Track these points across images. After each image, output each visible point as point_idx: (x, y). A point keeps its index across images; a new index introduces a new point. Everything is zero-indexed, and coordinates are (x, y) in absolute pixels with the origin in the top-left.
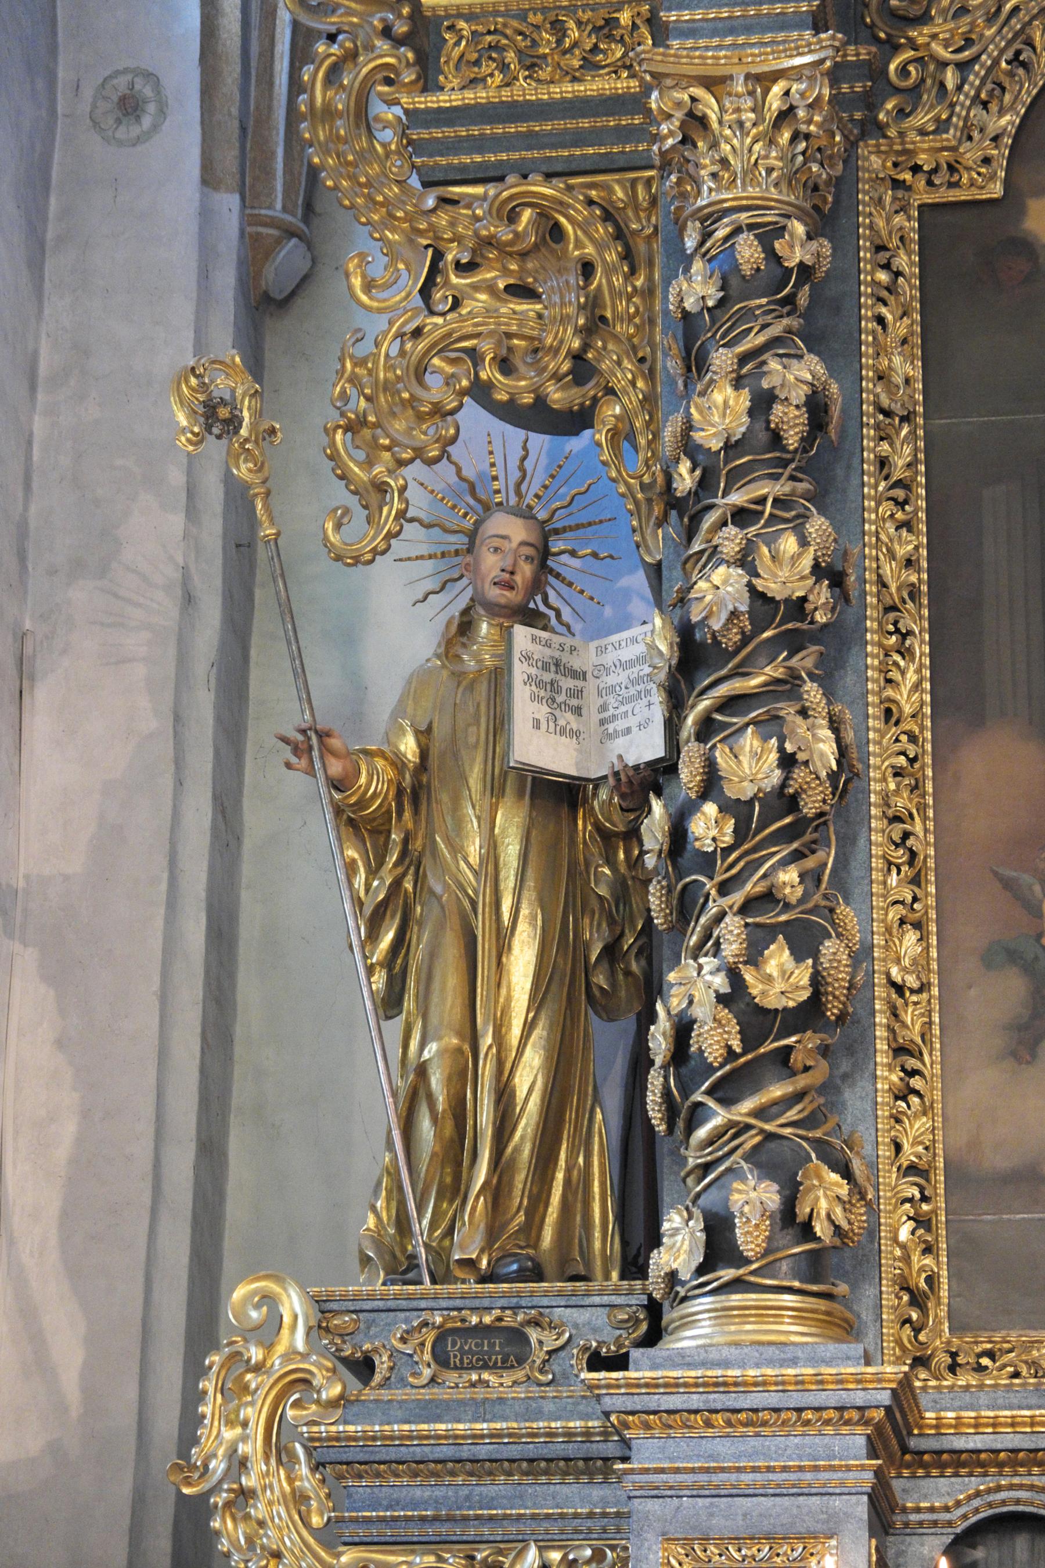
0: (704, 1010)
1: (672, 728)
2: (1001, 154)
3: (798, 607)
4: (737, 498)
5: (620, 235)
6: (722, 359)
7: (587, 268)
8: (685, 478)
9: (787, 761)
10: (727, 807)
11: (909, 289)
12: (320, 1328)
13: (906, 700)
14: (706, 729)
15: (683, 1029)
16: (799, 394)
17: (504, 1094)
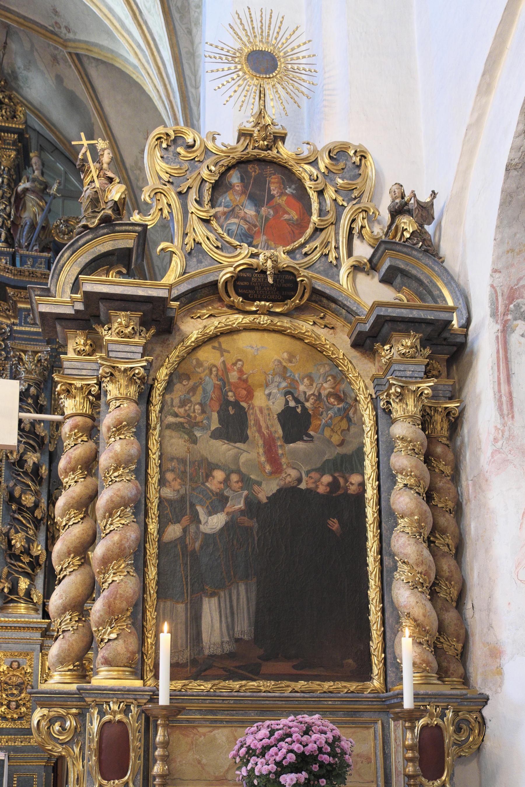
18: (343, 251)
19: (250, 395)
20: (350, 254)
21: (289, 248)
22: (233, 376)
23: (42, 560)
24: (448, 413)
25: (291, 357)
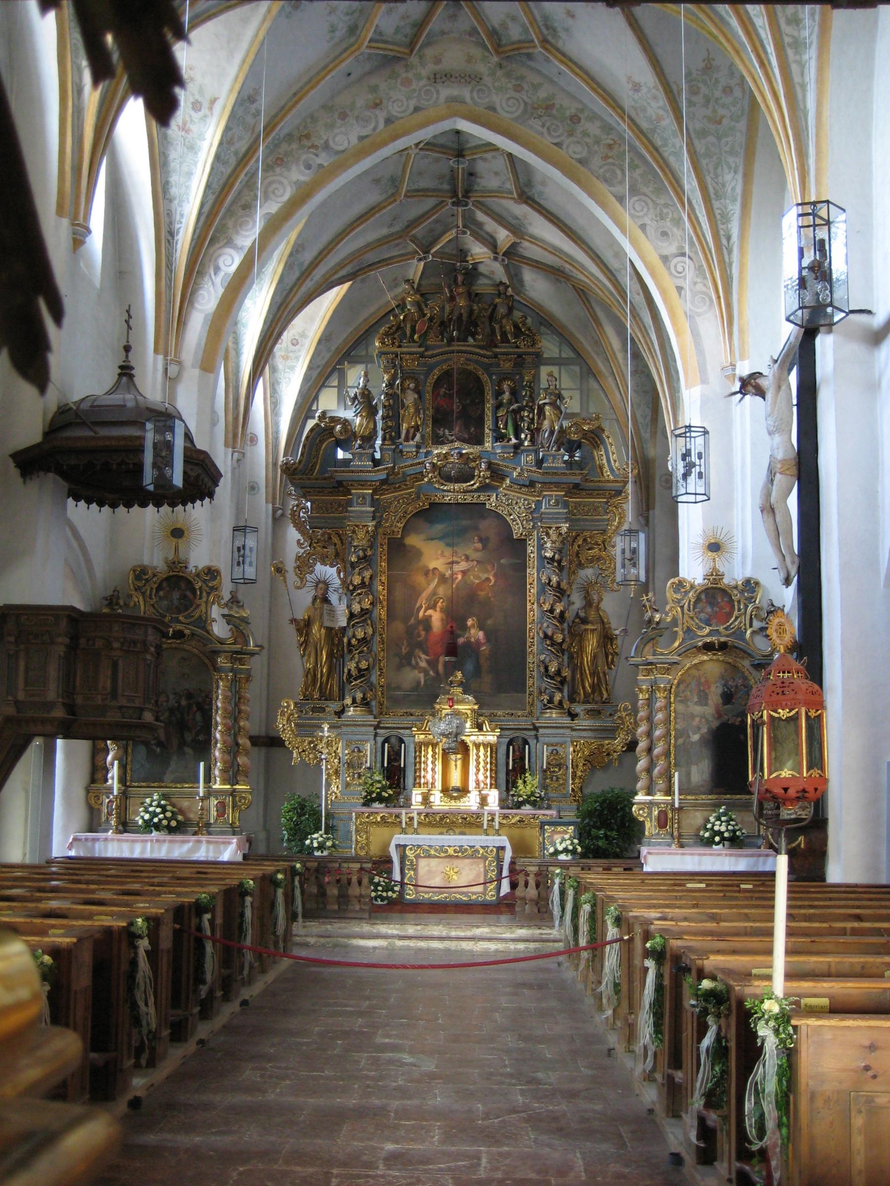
0: (353, 669)
1: (348, 623)
2: (400, 531)
5: (341, 539)
6: (357, 569)
7: (335, 545)
8: (351, 588)
9: (365, 633)
11: (386, 552)
12: (295, 706)
13: (383, 617)
14: (353, 625)
17: (322, 671)
18: (748, 625)
19: (709, 687)
22: (703, 680)
23: (569, 679)
25: (726, 671)
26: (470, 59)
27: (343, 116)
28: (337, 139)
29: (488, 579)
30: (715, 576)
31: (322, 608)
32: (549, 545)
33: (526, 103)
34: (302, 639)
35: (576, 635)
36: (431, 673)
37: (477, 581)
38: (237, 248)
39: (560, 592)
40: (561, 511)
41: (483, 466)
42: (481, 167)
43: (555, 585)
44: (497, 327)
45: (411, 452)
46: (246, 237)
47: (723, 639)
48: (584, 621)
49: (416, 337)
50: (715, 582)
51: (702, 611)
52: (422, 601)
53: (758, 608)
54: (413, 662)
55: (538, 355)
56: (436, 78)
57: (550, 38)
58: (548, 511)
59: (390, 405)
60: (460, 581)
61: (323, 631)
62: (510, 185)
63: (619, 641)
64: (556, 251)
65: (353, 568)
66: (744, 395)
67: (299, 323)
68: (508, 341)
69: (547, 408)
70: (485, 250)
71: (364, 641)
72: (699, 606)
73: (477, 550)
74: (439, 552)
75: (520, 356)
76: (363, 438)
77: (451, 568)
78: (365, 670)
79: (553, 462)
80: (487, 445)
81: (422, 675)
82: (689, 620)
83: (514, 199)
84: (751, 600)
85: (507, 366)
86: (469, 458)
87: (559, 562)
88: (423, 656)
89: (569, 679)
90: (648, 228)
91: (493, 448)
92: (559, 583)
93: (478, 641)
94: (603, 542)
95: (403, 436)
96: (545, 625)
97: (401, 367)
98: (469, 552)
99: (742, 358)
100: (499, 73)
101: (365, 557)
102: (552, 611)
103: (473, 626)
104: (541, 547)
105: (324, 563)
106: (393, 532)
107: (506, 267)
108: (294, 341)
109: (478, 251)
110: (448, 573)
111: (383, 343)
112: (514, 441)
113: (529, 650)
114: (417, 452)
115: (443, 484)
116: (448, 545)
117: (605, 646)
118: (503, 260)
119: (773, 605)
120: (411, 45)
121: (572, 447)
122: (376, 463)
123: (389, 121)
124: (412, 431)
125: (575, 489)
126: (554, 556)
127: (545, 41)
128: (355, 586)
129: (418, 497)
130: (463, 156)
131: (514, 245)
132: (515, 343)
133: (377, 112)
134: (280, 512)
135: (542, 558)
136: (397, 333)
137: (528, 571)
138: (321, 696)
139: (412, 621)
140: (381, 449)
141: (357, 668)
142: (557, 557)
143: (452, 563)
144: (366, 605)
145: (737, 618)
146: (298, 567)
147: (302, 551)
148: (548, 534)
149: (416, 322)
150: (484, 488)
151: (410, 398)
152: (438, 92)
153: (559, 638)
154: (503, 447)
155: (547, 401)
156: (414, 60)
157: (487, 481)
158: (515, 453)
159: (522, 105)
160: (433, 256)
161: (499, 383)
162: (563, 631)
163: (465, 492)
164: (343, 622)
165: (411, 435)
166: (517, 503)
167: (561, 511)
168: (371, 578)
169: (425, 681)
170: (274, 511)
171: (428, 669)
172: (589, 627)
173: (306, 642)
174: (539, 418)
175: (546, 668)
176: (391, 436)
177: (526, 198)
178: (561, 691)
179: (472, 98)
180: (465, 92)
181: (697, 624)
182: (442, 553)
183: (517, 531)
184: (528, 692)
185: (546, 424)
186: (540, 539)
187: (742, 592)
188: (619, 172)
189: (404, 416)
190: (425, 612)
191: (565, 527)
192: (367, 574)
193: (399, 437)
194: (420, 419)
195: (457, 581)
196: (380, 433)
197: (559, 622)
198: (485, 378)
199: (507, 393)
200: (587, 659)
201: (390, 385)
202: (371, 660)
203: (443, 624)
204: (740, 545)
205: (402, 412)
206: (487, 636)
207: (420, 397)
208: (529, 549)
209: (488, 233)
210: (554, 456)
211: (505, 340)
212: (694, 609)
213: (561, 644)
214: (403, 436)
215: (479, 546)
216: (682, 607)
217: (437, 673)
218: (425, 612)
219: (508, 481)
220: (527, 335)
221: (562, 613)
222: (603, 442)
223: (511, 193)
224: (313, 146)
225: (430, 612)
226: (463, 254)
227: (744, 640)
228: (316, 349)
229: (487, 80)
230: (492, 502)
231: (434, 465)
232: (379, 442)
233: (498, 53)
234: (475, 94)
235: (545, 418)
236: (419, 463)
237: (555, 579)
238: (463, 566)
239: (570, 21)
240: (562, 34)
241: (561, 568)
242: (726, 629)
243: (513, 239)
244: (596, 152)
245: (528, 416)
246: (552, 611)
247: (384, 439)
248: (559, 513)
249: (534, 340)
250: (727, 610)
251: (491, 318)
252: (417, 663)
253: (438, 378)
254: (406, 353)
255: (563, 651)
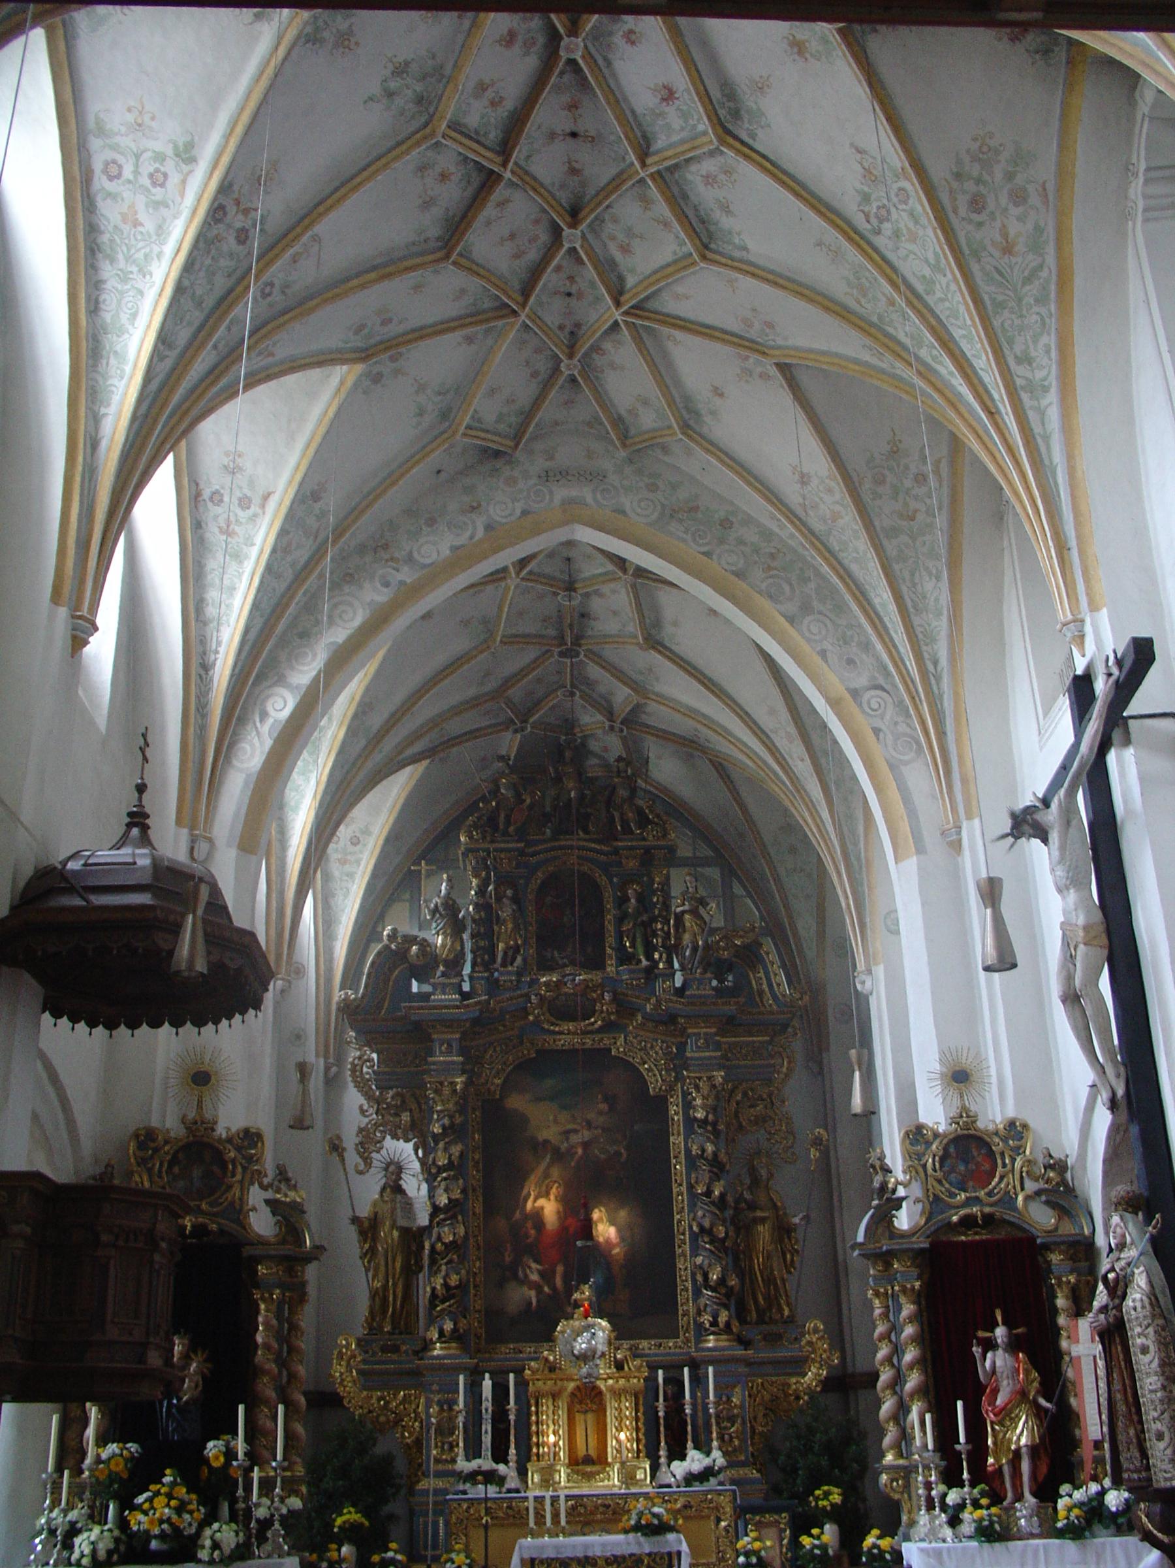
0: (438, 1287)
1: (431, 1221)
3: (457, 1200)
4: (444, 1175)
6: (441, 1145)
8: (434, 1171)
10: (443, 1243)
13: (477, 1211)
14: (438, 1224)
15: (434, 1289)
16: (457, 1154)
18: (1018, 1188)
20: (1022, 1189)
21: (986, 1190)
24: (1088, 1282)
26: (590, 455)
27: (431, 522)
28: (423, 552)
29: (618, 1154)
30: (965, 1119)
31: (393, 1201)
32: (699, 1102)
33: (663, 505)
34: (367, 1246)
35: (743, 1226)
36: (546, 1289)
37: (603, 1156)
38: (289, 686)
39: (717, 1168)
40: (713, 1054)
41: (607, 996)
42: (596, 605)
43: (710, 1158)
44: (617, 815)
45: (511, 981)
46: (301, 672)
47: (987, 1210)
48: (752, 1206)
49: (511, 829)
50: (967, 1126)
51: (953, 1170)
52: (531, 1188)
53: (1029, 1161)
54: (521, 1274)
55: (672, 850)
56: (547, 476)
57: (691, 423)
58: (696, 1055)
59: (481, 919)
60: (581, 1157)
61: (396, 1234)
62: (633, 628)
63: (799, 1234)
64: (691, 713)
65: (436, 1143)
66: (1017, 838)
67: (359, 813)
68: (632, 832)
69: (687, 916)
70: (600, 717)
71: (451, 1246)
72: (948, 1162)
73: (601, 1113)
74: (551, 1118)
75: (647, 850)
76: (447, 963)
77: (567, 1139)
78: (456, 1287)
79: (698, 989)
80: (609, 969)
81: (533, 1293)
82: (935, 1184)
83: (638, 644)
84: (1018, 1150)
85: (632, 864)
86: (587, 986)
87: (715, 1124)
88: (534, 1265)
89: (737, 1289)
90: (829, 654)
91: (617, 972)
92: (715, 1154)
93: (608, 1241)
94: (770, 1095)
95: (499, 960)
96: (700, 1213)
97: (495, 868)
98: (591, 1116)
99: (969, 817)
100: (628, 470)
101: (452, 1125)
102: (709, 1193)
103: (601, 1220)
104: (688, 1105)
105: (395, 1137)
106: (489, 1089)
107: (624, 740)
108: (355, 840)
109: (590, 719)
110: (564, 1146)
111: (471, 837)
112: (645, 963)
113: (678, 1251)
114: (519, 981)
115: (553, 1024)
116: (564, 1107)
117: (781, 1241)
118: (622, 731)
119: (1051, 1156)
120: (517, 438)
121: (720, 968)
122: (465, 996)
123: (489, 528)
124: (510, 953)
125: (729, 1024)
126: (707, 1117)
127: (685, 427)
128: (439, 1168)
129: (522, 1043)
130: (575, 590)
131: (637, 709)
132: (642, 833)
133: (474, 516)
134: (334, 1069)
135: (690, 1121)
136: (490, 825)
137: (672, 1139)
138: (394, 1328)
139: (518, 1215)
140: (471, 978)
141: (446, 1285)
142: (711, 1117)
143: (568, 1132)
144: (457, 1194)
145: (1002, 1178)
146: (361, 1143)
147: (367, 1120)
148: (697, 1088)
149: (512, 810)
150: (609, 1027)
151: (506, 912)
152: (551, 493)
153: (721, 1231)
154: (631, 972)
155: (686, 907)
156: (518, 454)
157: (612, 1018)
158: (647, 979)
159: (659, 507)
160: (532, 727)
161: (623, 887)
162: (724, 1221)
163: (585, 1033)
164: (423, 1219)
165: (509, 959)
166: (652, 1047)
167: (713, 1054)
168: (462, 1154)
169: (538, 1301)
170: (327, 1069)
171: (541, 1283)
172: (759, 1214)
173: (373, 1251)
174: (677, 930)
175: (706, 1276)
176: (483, 959)
177: (654, 641)
178: (726, 1307)
179: (595, 500)
180: (586, 493)
181: (948, 1190)
182: (556, 1121)
183: (655, 1083)
184: (680, 1312)
185: (687, 938)
186: (685, 1094)
187: (1005, 1140)
188: (787, 588)
189: (499, 933)
190: (535, 1201)
191: (719, 1076)
192: (456, 1150)
193: (494, 962)
194: (521, 936)
195: (577, 1157)
196: (469, 957)
197: (720, 1210)
198: (603, 880)
199: (633, 901)
200: (758, 1261)
201: (481, 892)
202: (463, 1272)
203: (559, 1218)
204: (993, 1071)
205: (496, 928)
206: (619, 1231)
207: (520, 908)
208: (673, 1109)
209: (601, 696)
210: (700, 981)
211: (627, 830)
212: (941, 1167)
213: (723, 1240)
214: (499, 960)
215: (603, 1107)
216: (924, 1166)
217: (554, 1288)
218: (535, 1201)
219: (639, 1018)
220: (657, 824)
221: (723, 1196)
222: (761, 961)
223: (636, 637)
224: (392, 559)
225: (542, 1202)
226: (569, 724)
227: (1015, 1209)
228: (382, 852)
229: (613, 479)
230: (619, 1046)
231: (542, 998)
232: (467, 970)
233: (624, 445)
234: (599, 496)
235: (684, 931)
236: (522, 996)
237: (710, 1148)
238: (586, 1135)
239: (718, 401)
240: (708, 419)
241: (716, 1133)
242: (990, 1194)
243: (635, 699)
244: (756, 563)
245: (662, 929)
246: (709, 1193)
247: (474, 964)
248: (710, 1058)
249: (665, 830)
250: (987, 1167)
251: (609, 802)
252: (526, 1276)
253: (543, 883)
254: (502, 850)
255: (726, 1250)
